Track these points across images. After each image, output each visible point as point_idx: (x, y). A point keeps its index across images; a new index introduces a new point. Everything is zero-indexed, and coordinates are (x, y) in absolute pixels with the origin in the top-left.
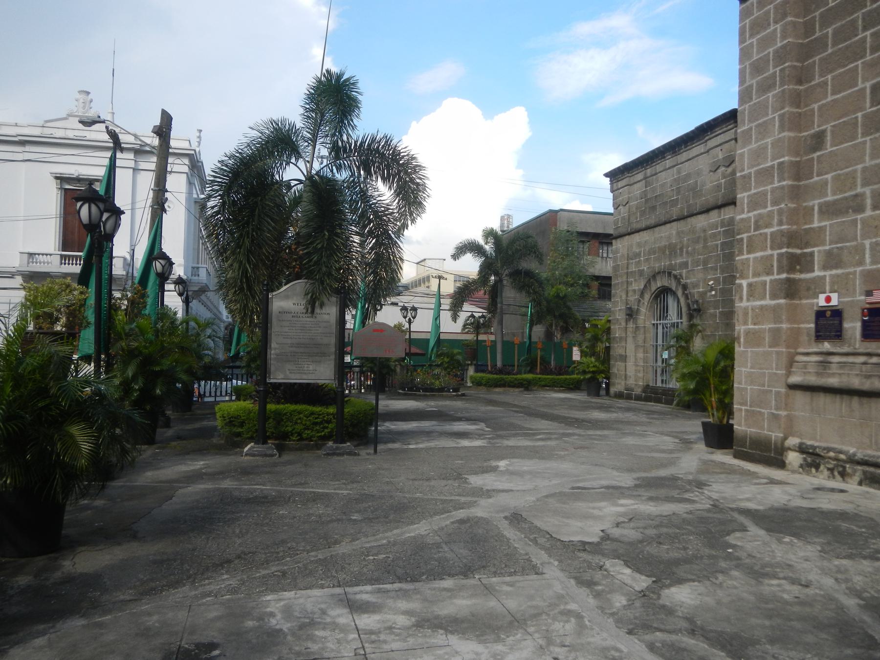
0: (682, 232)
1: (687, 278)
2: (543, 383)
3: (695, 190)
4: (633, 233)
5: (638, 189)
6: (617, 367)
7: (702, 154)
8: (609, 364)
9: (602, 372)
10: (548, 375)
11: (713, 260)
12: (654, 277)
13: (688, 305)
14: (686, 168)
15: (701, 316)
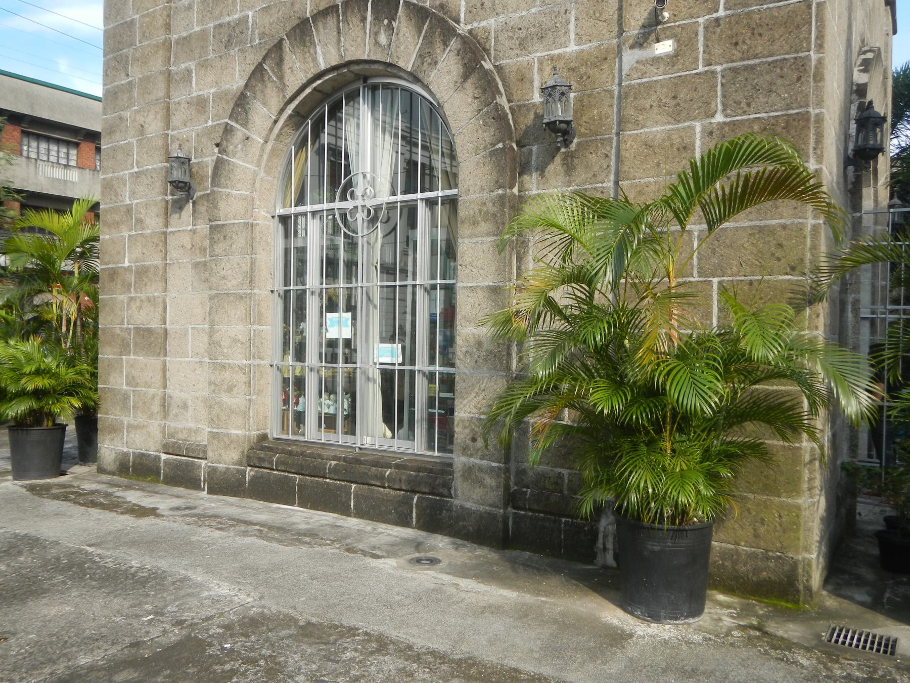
8: (95, 361)
9: (72, 390)
13: (499, 117)
15: (570, 156)
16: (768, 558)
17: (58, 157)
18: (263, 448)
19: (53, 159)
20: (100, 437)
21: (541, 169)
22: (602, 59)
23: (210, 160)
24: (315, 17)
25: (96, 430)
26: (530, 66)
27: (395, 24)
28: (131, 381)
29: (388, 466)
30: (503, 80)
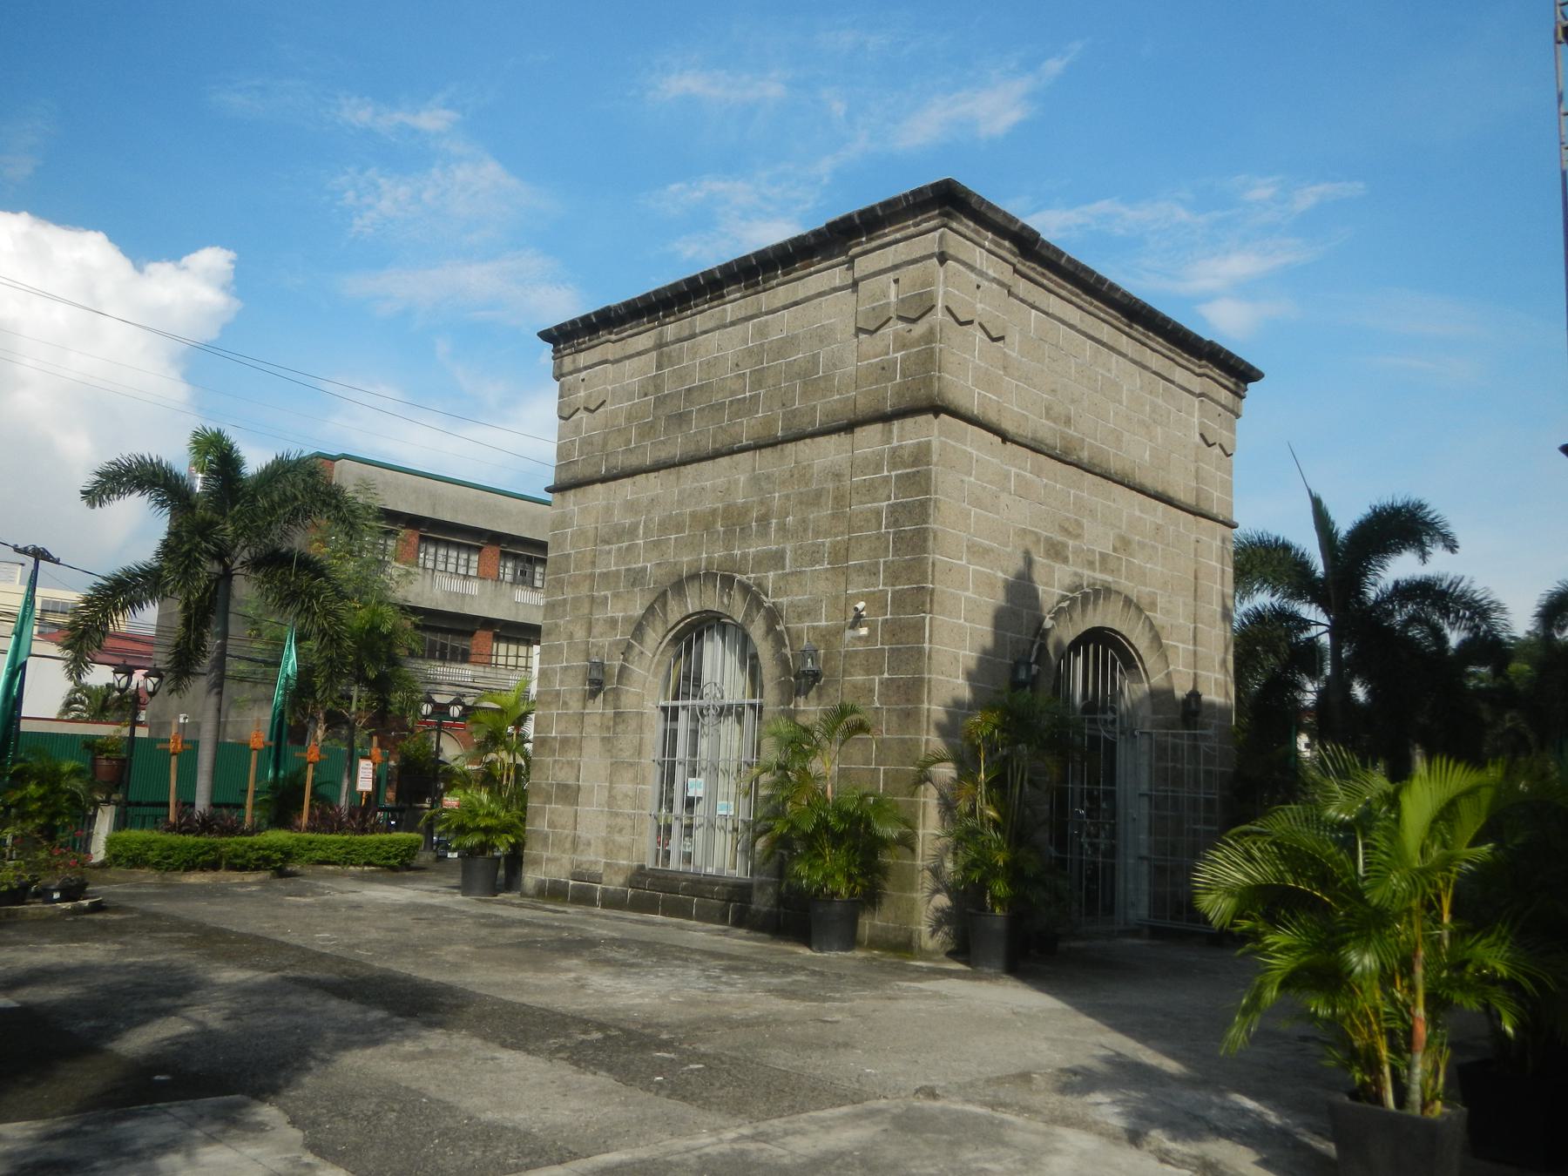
0: (768, 477)
1: (778, 591)
2: (319, 855)
3: (810, 378)
4: (615, 478)
5: (635, 373)
6: (546, 818)
7: (835, 290)
8: (524, 809)
9: (508, 829)
10: (331, 832)
11: (866, 547)
12: (679, 586)
13: (783, 662)
14: (783, 325)
15: (820, 689)
16: (900, 929)
17: (457, 565)
18: (640, 875)
19: (451, 568)
20: (524, 868)
21: (806, 694)
22: (838, 632)
23: (617, 663)
24: (687, 578)
25: (521, 863)
26: (803, 629)
27: (732, 593)
28: (552, 825)
29: (717, 885)
30: (789, 636)
